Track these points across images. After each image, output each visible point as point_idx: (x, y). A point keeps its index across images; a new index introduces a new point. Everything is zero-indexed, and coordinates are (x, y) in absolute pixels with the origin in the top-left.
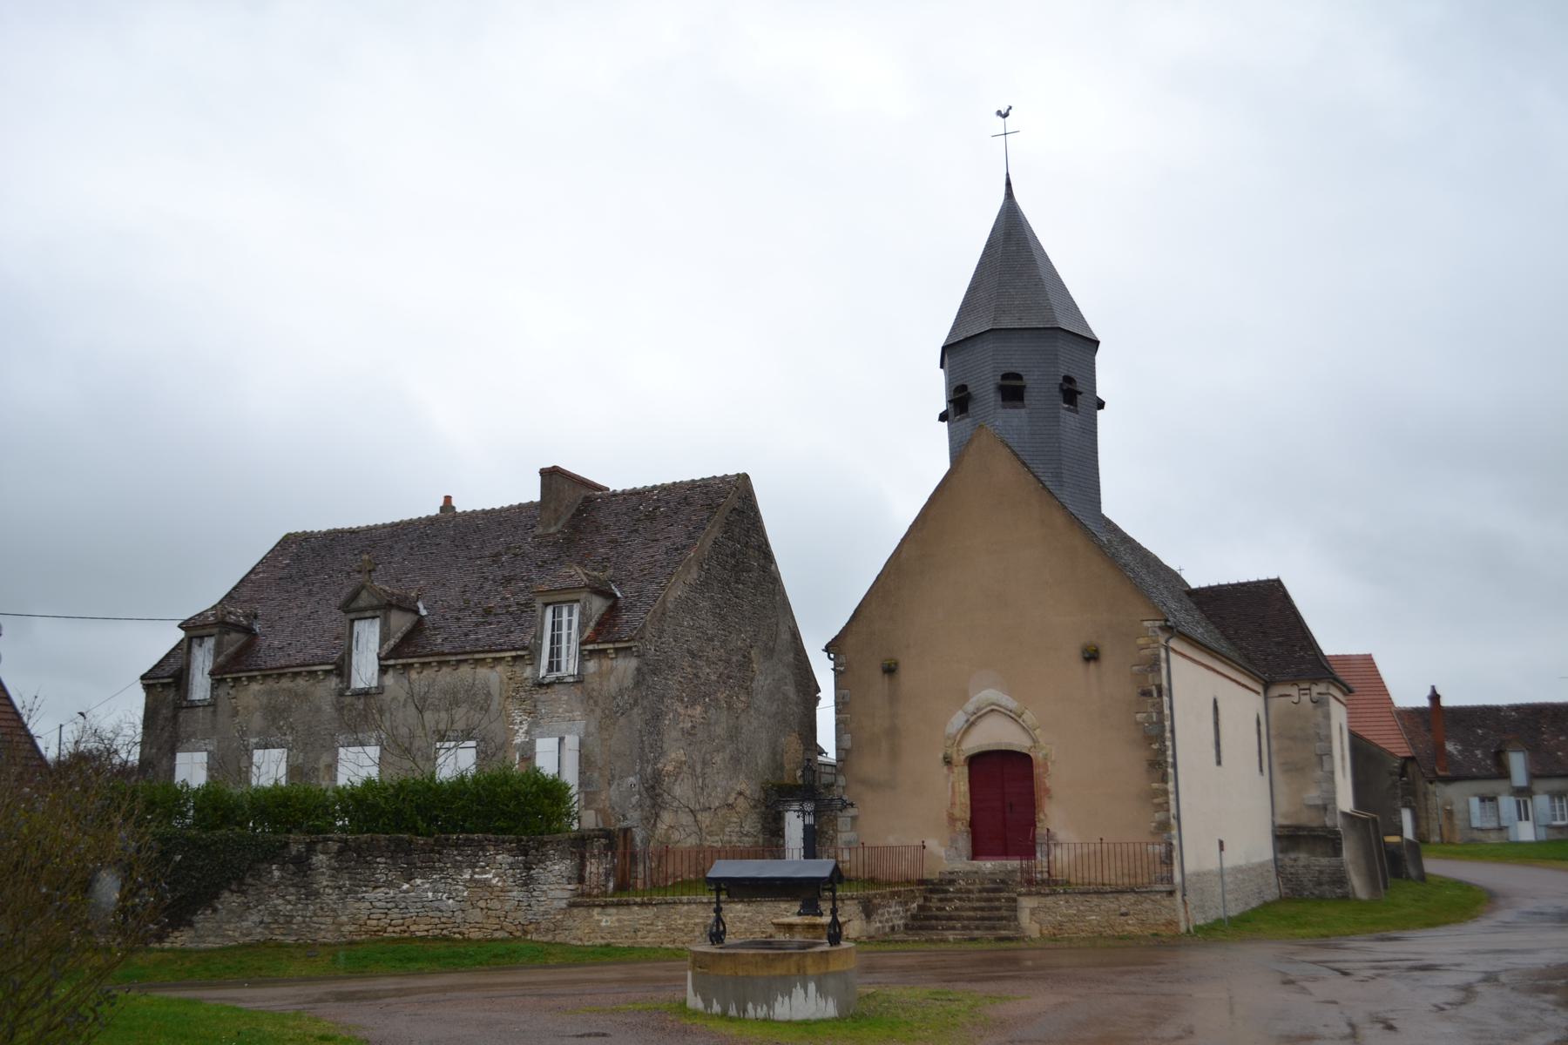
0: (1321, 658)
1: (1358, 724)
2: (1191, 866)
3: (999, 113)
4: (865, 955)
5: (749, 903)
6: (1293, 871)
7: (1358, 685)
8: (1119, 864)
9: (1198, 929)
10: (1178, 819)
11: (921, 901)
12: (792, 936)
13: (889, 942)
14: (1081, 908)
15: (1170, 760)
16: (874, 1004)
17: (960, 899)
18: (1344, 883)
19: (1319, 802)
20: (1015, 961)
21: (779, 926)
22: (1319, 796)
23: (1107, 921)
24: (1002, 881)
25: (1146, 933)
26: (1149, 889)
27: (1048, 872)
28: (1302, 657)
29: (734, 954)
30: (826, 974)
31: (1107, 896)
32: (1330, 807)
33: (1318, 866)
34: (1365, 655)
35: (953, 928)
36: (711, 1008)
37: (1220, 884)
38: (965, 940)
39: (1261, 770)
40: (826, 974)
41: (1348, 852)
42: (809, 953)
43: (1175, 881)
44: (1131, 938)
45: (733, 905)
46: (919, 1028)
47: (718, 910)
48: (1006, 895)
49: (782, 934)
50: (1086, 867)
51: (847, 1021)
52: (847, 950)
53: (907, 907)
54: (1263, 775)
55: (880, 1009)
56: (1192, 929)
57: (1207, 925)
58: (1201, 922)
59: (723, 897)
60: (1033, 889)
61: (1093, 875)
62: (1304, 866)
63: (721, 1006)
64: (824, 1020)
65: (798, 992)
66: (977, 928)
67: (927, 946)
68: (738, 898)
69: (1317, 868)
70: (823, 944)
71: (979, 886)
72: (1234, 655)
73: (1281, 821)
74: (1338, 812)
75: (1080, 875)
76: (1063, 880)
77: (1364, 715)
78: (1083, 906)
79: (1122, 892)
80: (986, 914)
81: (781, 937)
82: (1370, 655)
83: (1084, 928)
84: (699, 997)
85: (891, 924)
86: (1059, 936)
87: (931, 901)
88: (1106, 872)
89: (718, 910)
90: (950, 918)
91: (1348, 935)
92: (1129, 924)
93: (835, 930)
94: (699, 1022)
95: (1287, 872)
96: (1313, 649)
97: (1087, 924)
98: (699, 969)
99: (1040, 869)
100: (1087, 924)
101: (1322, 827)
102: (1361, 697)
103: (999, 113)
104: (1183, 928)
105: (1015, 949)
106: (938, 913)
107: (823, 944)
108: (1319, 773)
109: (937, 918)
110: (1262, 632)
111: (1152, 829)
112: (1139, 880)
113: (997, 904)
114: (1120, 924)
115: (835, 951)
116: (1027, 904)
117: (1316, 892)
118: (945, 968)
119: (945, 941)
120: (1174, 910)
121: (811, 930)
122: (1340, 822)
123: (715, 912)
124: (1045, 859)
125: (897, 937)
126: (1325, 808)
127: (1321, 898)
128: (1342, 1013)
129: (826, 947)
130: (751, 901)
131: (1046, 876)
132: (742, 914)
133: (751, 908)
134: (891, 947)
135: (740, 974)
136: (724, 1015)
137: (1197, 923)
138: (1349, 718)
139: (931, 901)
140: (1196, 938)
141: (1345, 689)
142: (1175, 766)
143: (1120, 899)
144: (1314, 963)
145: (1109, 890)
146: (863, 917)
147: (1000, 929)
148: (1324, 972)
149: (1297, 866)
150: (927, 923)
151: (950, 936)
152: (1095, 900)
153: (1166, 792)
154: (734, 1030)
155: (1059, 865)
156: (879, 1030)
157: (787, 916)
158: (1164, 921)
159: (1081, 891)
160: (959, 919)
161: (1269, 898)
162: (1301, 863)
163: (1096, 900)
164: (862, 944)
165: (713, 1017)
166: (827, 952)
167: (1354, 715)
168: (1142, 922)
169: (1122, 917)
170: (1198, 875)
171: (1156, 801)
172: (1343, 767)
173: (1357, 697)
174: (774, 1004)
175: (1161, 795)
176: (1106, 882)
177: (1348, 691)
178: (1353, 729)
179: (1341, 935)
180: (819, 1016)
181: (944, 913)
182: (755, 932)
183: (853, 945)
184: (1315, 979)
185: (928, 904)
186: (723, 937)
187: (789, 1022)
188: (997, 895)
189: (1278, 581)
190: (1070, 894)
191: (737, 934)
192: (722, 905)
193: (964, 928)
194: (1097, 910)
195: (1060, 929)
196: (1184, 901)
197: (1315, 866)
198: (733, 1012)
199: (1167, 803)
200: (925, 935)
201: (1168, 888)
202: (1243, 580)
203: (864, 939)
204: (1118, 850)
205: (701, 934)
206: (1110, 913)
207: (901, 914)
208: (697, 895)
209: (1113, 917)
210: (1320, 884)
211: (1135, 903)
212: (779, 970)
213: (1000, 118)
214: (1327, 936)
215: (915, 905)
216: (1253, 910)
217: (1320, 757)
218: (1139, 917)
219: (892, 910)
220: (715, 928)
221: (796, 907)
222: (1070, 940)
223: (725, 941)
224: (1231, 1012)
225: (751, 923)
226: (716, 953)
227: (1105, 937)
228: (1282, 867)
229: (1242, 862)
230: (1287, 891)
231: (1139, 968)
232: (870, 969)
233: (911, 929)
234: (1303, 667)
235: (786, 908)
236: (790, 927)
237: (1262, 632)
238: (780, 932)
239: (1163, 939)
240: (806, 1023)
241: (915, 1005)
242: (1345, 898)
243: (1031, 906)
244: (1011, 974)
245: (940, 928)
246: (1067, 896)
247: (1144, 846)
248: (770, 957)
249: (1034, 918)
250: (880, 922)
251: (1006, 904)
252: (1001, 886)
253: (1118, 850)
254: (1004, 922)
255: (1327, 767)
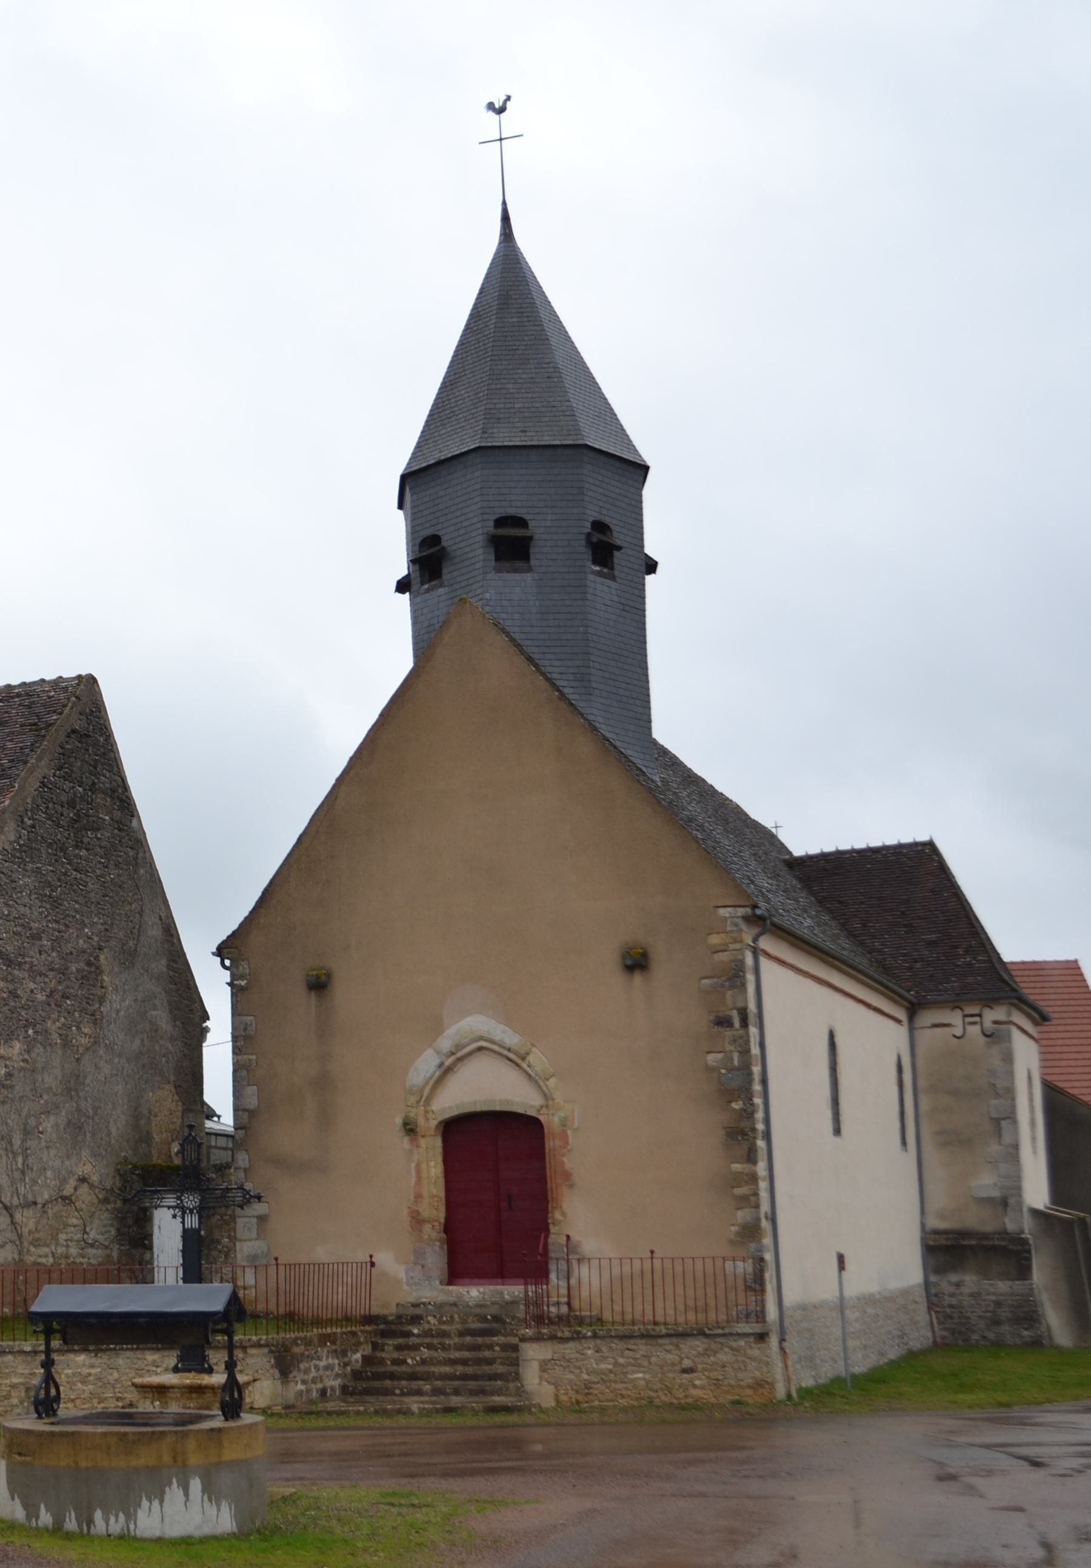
0: (998, 966)
1: (1056, 1070)
2: (791, 1296)
3: (491, 106)
4: (280, 1435)
5: (97, 1352)
6: (954, 1301)
7: (1057, 1009)
8: (680, 1290)
9: (806, 1393)
10: (773, 1219)
11: (367, 1350)
12: (165, 1404)
13: (318, 1414)
14: (621, 1360)
15: (760, 1127)
16: (293, 1511)
17: (429, 1347)
18: (1034, 1321)
19: (996, 1193)
20: (516, 1445)
21: (143, 1388)
22: (995, 1185)
23: (661, 1381)
24: (497, 1319)
25: (722, 1400)
26: (727, 1331)
27: (569, 1304)
28: (969, 964)
29: (73, 1433)
30: (219, 1465)
31: (660, 1341)
32: (1012, 1201)
33: (995, 1294)
34: (1067, 962)
35: (419, 1392)
36: (37, 1518)
37: (839, 1323)
38: (437, 1411)
39: (904, 1142)
40: (219, 1465)
41: (1039, 1275)
42: (191, 1431)
43: (768, 1319)
44: (698, 1408)
45: (71, 1356)
46: (365, 1550)
47: (48, 1364)
48: (502, 1339)
49: (148, 1402)
50: (627, 1296)
51: (252, 1538)
52: (252, 1426)
53: (346, 1360)
54: (906, 1150)
55: (303, 1520)
56: (794, 1394)
57: (818, 1387)
58: (808, 1382)
59: (55, 1343)
60: (545, 1331)
61: (638, 1307)
62: (972, 1295)
63: (53, 1515)
64: (215, 1538)
65: (174, 1493)
66: (457, 1392)
67: (379, 1420)
68: (78, 1344)
69: (993, 1298)
70: (213, 1416)
71: (459, 1327)
72: (862, 961)
73: (934, 1223)
74: (1025, 1210)
75: (618, 1308)
76: (591, 1317)
77: (1064, 1056)
78: (622, 1357)
79: (684, 1335)
80: (470, 1370)
81: (146, 1406)
82: (1076, 961)
83: (624, 1392)
84: (17, 1500)
85: (320, 1386)
86: (586, 1405)
87: (383, 1350)
88: (659, 1304)
89: (48, 1364)
90: (413, 1377)
91: (1041, 1403)
92: (695, 1387)
93: (232, 1395)
94: (17, 1540)
95: (946, 1303)
96: (986, 952)
97: (630, 1386)
98: (18, 1458)
99: (556, 1299)
100: (630, 1386)
101: (999, 1233)
102: (1060, 1028)
103: (491, 106)
104: (780, 1392)
105: (516, 1426)
106: (395, 1368)
107: (213, 1416)
108: (994, 1148)
109: (392, 1376)
110: (906, 926)
111: (732, 1237)
112: (712, 1316)
113: (487, 1354)
114: (680, 1386)
115: (232, 1428)
116: (534, 1354)
117: (991, 1335)
118: (406, 1455)
119: (406, 1412)
120: (767, 1364)
121: (194, 1395)
122: (1027, 1224)
123: (42, 1367)
124: (563, 1284)
125: (330, 1406)
126: (1004, 1203)
127: (998, 1345)
128: (1031, 1526)
129: (218, 1423)
130: (102, 1350)
131: (564, 1309)
132: (85, 1371)
133: (100, 1361)
134: (321, 1422)
135: (83, 1464)
136: (58, 1529)
137: (803, 1385)
138: (1042, 1060)
139: (383, 1350)
140: (801, 1408)
141: (1036, 1016)
142: (767, 1136)
143: (682, 1346)
144: (988, 1446)
145: (664, 1331)
146: (277, 1374)
147: (492, 1394)
148: (1002, 1461)
149: (961, 1294)
150: (377, 1384)
151: (414, 1404)
152: (642, 1347)
153: (754, 1178)
154: (73, 1552)
155: (585, 1293)
156: (302, 1552)
157: (157, 1374)
158: (750, 1381)
159: (621, 1334)
160: (427, 1377)
161: (915, 1345)
162: (967, 1291)
163: (644, 1348)
164: (275, 1419)
165: (39, 1532)
166: (219, 1430)
167: (1050, 1056)
168: (717, 1384)
169: (685, 1376)
170: (803, 1308)
171: (738, 1191)
172: (1034, 1139)
173: (1053, 1028)
174: (136, 1512)
175: (747, 1183)
176: (660, 1318)
177: (1041, 1018)
178: (1048, 1078)
179: (1029, 1403)
180: (207, 1530)
181: (404, 1368)
182: (106, 1399)
183: (260, 1418)
184: (989, 1473)
185: (379, 1354)
186: (55, 1407)
187: (159, 1540)
188: (488, 1340)
189: (931, 845)
190: (602, 1338)
191: (78, 1402)
192: (55, 1356)
193: (436, 1392)
194: (646, 1363)
195: (587, 1394)
196: (782, 1349)
197: (988, 1294)
198: (71, 1524)
199: (756, 1194)
200: (374, 1403)
201: (757, 1328)
202: (876, 843)
203: (278, 1409)
204: (679, 1269)
205: (22, 1402)
206: (665, 1368)
207: (336, 1369)
208: (14, 1340)
209: (671, 1375)
210: (997, 1322)
211: (706, 1353)
212: (145, 1458)
213: (492, 114)
214: (1007, 1405)
215: (358, 1356)
216: (892, 1363)
217: (997, 1122)
218: (714, 1374)
219: (322, 1363)
220: (43, 1392)
221: (171, 1359)
222: (603, 1410)
223: (59, 1412)
224: (857, 1523)
225: (100, 1384)
226: (44, 1432)
227: (658, 1407)
228: (936, 1295)
229: (873, 1288)
230: (945, 1333)
231: (712, 1455)
232: (287, 1456)
233: (352, 1394)
234: (970, 980)
235: (155, 1361)
236: (161, 1391)
237: (906, 926)
238: (145, 1398)
239: (751, 1410)
240: (186, 1542)
241: (359, 1513)
242: (1037, 1344)
243: (542, 1358)
244: (509, 1464)
245: (398, 1392)
246: (598, 1341)
247: (719, 1263)
248: (131, 1437)
249: (546, 1376)
250: (304, 1382)
251: (502, 1354)
252: (495, 1325)
253: (679, 1269)
254: (499, 1382)
255: (1007, 1139)
